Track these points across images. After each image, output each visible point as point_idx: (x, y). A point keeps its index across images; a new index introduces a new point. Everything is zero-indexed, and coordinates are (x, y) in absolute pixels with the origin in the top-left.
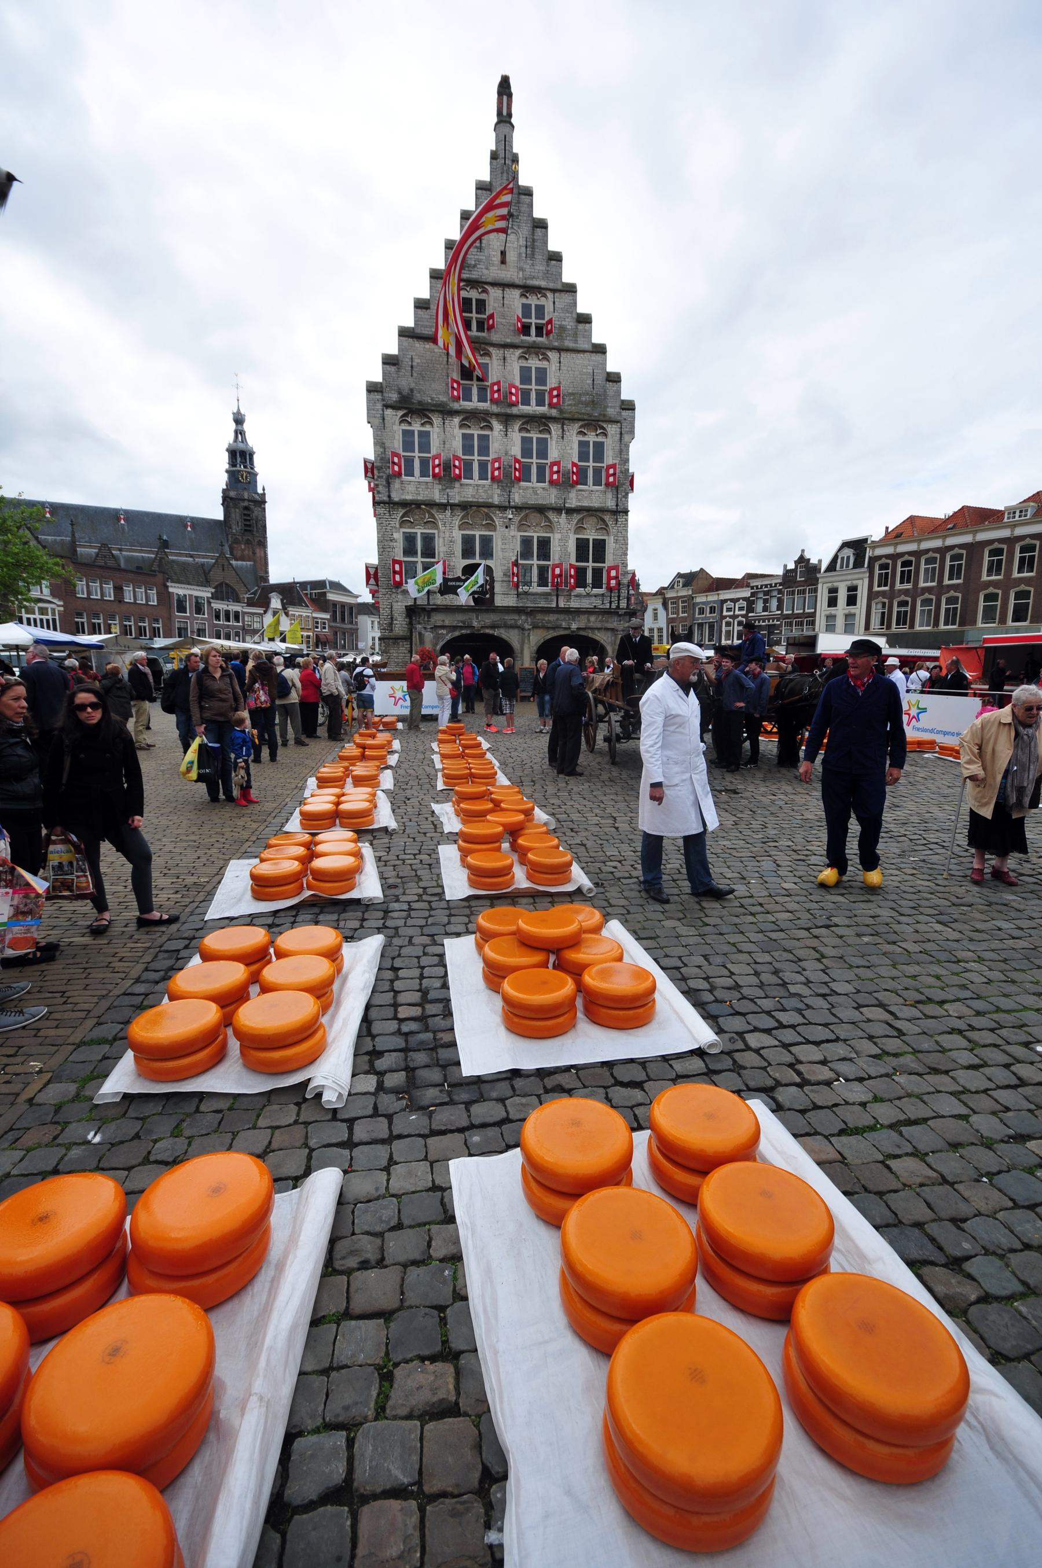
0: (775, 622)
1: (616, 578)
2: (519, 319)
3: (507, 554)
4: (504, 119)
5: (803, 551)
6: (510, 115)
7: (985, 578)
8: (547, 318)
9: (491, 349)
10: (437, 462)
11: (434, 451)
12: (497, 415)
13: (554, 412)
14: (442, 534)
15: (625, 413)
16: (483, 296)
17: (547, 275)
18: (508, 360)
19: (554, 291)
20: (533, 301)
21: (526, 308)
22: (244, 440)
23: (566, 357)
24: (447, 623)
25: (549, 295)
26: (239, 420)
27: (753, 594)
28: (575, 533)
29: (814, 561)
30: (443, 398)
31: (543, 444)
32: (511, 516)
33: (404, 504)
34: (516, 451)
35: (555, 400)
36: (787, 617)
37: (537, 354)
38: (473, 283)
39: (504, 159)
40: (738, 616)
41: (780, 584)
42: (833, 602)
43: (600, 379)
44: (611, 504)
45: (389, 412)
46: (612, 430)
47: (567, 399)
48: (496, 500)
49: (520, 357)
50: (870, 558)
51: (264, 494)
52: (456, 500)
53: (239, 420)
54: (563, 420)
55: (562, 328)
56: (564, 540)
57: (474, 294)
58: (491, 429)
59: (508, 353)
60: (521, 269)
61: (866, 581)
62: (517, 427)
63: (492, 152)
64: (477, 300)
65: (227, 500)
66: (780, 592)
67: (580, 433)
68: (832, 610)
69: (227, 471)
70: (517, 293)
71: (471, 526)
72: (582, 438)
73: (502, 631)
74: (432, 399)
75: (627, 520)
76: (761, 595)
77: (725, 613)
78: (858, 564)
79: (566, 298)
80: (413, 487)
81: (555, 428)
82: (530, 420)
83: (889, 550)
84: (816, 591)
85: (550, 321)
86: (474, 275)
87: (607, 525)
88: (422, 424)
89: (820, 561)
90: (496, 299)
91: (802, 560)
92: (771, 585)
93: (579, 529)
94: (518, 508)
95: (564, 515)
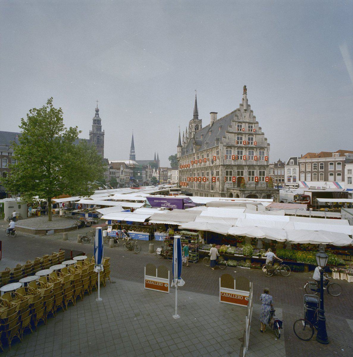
7: (329, 170)
19: (254, 123)
20: (250, 125)
22: (98, 117)
23: (257, 136)
25: (254, 124)
26: (97, 111)
29: (283, 162)
43: (263, 139)
52: (236, 164)
53: (97, 111)
58: (243, 149)
61: (298, 168)
71: (239, 169)
78: (296, 164)
81: (255, 149)
86: (240, 121)
93: (259, 169)
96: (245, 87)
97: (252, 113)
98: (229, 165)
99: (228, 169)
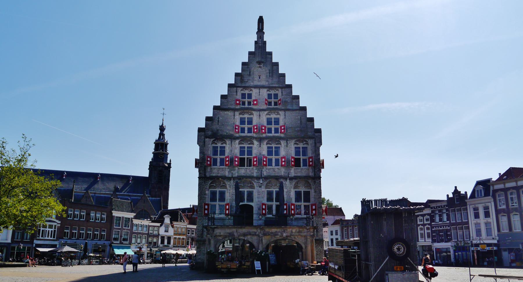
0: (447, 228)
1: (315, 210)
2: (266, 100)
3: (260, 200)
4: (260, 31)
5: (456, 187)
6: (263, 29)
8: (279, 98)
9: (253, 112)
10: (227, 159)
11: (226, 155)
12: (256, 138)
13: (282, 135)
14: (228, 191)
15: (316, 134)
16: (251, 92)
17: (278, 82)
18: (261, 116)
19: (282, 88)
20: (272, 92)
21: (270, 96)
23: (288, 113)
24: (222, 234)
25: (280, 90)
26: (162, 128)
27: (432, 212)
28: (294, 188)
29: (463, 192)
30: (231, 133)
31: (278, 149)
32: (261, 182)
33: (212, 178)
34: (265, 152)
35: (283, 131)
36: (453, 224)
37: (275, 113)
38: (245, 88)
39: (260, 44)
40: (426, 225)
41: (447, 206)
42: (477, 216)
43: (304, 121)
44: (311, 174)
45: (207, 140)
46: (310, 142)
47: (288, 130)
48: (255, 175)
49: (267, 114)
50: (493, 191)
51: (170, 164)
52: (236, 175)
53: (162, 128)
54: (287, 139)
55: (286, 102)
56: (289, 192)
57: (247, 92)
58: (253, 144)
59: (261, 113)
60: (267, 81)
62: (265, 143)
63: (255, 41)
64: (248, 94)
65: (153, 166)
66: (447, 210)
67: (295, 144)
68: (477, 220)
69: (153, 153)
70: (265, 90)
72: (296, 146)
73: (249, 237)
74: (227, 133)
75: (320, 182)
76: (437, 212)
77: (419, 223)
78: (487, 194)
79: (287, 90)
80: (216, 170)
81: (283, 143)
82: (271, 140)
83: (501, 186)
84: (466, 209)
85: (280, 100)
86: (247, 85)
87: (310, 185)
88: (222, 144)
89: (466, 192)
90: (256, 93)
91: (456, 192)
92: (441, 206)
94: (266, 178)
95: (288, 180)
96: (261, 20)
97: (275, 67)
98: (217, 177)
99: (215, 187)
